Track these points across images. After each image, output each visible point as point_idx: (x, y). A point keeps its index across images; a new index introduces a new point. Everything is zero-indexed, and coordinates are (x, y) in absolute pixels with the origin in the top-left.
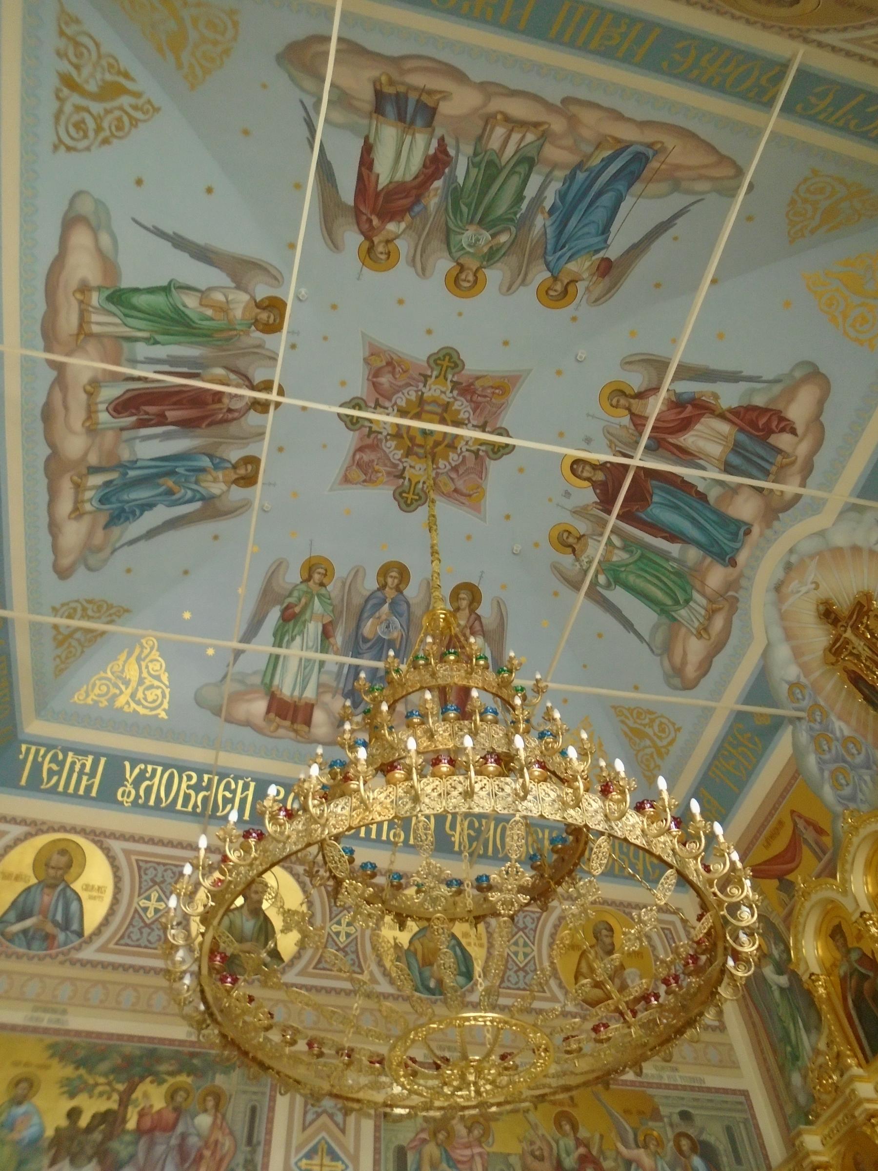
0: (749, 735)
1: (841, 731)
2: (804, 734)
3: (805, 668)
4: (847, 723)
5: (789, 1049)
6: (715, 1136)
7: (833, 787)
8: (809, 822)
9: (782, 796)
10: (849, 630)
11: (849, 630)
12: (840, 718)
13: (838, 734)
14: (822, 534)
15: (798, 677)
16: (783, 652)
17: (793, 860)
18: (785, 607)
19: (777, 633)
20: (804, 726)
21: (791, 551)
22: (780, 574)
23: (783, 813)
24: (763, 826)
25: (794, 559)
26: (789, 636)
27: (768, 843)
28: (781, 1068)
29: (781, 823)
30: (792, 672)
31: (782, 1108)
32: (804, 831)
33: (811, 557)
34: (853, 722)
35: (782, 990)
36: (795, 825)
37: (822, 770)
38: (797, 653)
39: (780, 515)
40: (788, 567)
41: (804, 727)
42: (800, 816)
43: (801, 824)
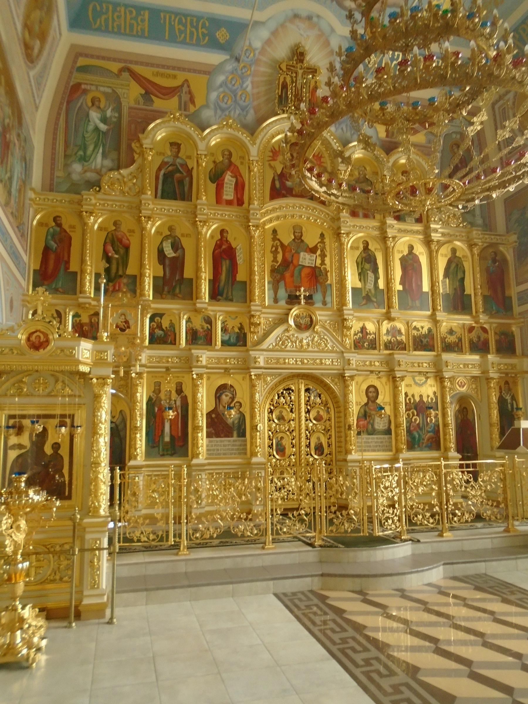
0: (206, 32)
1: (247, 86)
2: (231, 67)
3: (263, 51)
4: (253, 88)
5: (81, 153)
6: (28, 159)
7: (218, 97)
8: (190, 92)
9: (189, 70)
10: (302, 71)
11: (302, 71)
12: (252, 83)
13: (245, 85)
14: (333, 30)
15: (257, 49)
16: (264, 33)
17: (164, 95)
18: (288, 24)
19: (272, 25)
20: (235, 64)
21: (318, 16)
22: (304, 14)
23: (181, 77)
24: (163, 67)
25: (315, 19)
26: (275, 33)
27: (157, 74)
28: (66, 156)
29: (175, 77)
30: (257, 44)
31: (52, 169)
32: (184, 92)
33: (320, 30)
34: (255, 91)
35: (97, 129)
36: (182, 86)
37: (221, 86)
38: (268, 42)
39: (334, 2)
40: (309, 18)
41: (234, 65)
42: (189, 86)
43: (185, 89)
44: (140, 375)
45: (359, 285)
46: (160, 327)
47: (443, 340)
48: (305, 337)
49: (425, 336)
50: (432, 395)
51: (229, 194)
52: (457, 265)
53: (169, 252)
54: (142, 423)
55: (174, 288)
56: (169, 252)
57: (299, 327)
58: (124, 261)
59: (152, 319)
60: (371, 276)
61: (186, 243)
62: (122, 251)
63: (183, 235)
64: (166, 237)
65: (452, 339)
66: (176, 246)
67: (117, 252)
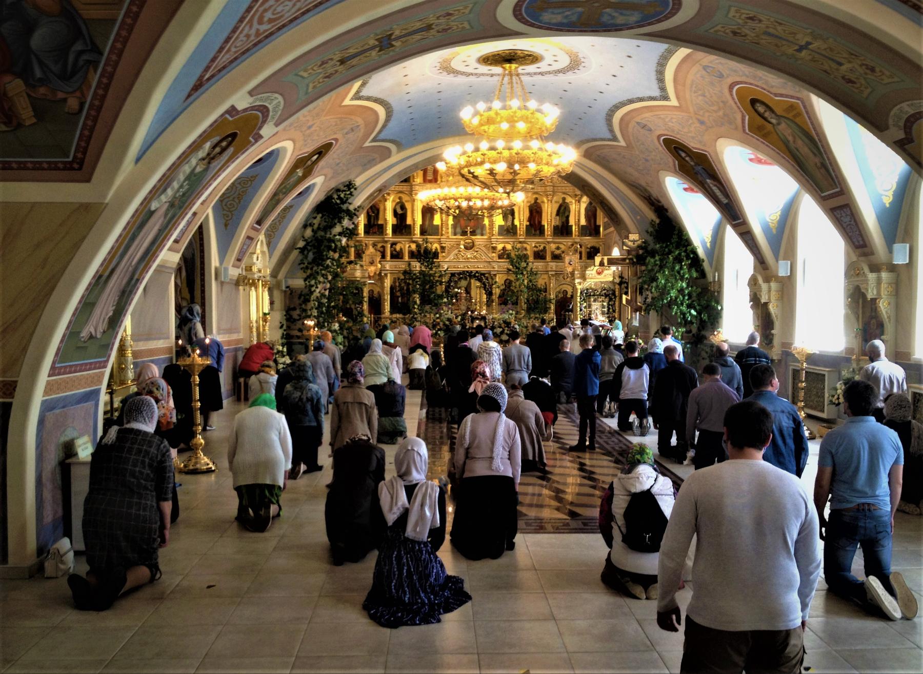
44: (386, 275)
45: (503, 223)
46: (395, 250)
47: (552, 253)
48: (469, 254)
49: (542, 251)
50: (543, 284)
51: (430, 176)
52: (565, 208)
53: (399, 211)
54: (388, 297)
55: (402, 230)
56: (399, 211)
57: (466, 248)
58: (377, 217)
59: (391, 247)
60: (510, 217)
61: (408, 206)
62: (376, 212)
63: (406, 201)
64: (398, 203)
65: (557, 252)
66: (403, 207)
67: (373, 213)
